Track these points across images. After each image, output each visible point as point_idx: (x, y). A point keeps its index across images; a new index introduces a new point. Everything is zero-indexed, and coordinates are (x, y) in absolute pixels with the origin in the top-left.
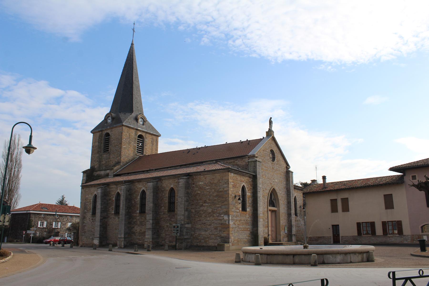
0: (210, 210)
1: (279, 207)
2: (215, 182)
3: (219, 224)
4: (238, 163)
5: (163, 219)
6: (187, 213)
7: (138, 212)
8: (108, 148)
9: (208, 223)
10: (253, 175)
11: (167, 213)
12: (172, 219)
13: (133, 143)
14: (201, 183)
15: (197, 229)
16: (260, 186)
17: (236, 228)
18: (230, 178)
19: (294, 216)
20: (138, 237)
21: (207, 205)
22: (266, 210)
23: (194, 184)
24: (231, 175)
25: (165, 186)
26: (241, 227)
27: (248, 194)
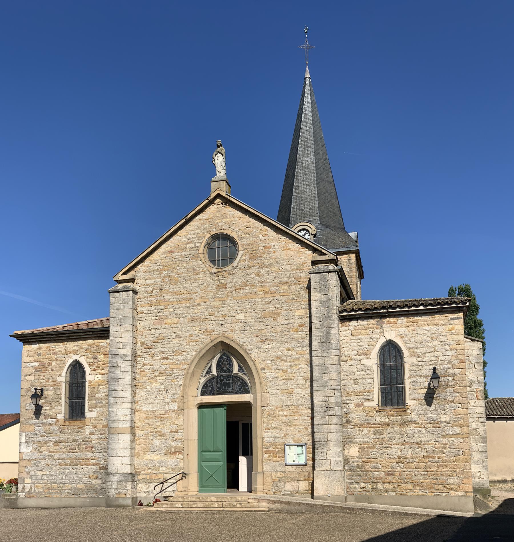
26: (64, 456)
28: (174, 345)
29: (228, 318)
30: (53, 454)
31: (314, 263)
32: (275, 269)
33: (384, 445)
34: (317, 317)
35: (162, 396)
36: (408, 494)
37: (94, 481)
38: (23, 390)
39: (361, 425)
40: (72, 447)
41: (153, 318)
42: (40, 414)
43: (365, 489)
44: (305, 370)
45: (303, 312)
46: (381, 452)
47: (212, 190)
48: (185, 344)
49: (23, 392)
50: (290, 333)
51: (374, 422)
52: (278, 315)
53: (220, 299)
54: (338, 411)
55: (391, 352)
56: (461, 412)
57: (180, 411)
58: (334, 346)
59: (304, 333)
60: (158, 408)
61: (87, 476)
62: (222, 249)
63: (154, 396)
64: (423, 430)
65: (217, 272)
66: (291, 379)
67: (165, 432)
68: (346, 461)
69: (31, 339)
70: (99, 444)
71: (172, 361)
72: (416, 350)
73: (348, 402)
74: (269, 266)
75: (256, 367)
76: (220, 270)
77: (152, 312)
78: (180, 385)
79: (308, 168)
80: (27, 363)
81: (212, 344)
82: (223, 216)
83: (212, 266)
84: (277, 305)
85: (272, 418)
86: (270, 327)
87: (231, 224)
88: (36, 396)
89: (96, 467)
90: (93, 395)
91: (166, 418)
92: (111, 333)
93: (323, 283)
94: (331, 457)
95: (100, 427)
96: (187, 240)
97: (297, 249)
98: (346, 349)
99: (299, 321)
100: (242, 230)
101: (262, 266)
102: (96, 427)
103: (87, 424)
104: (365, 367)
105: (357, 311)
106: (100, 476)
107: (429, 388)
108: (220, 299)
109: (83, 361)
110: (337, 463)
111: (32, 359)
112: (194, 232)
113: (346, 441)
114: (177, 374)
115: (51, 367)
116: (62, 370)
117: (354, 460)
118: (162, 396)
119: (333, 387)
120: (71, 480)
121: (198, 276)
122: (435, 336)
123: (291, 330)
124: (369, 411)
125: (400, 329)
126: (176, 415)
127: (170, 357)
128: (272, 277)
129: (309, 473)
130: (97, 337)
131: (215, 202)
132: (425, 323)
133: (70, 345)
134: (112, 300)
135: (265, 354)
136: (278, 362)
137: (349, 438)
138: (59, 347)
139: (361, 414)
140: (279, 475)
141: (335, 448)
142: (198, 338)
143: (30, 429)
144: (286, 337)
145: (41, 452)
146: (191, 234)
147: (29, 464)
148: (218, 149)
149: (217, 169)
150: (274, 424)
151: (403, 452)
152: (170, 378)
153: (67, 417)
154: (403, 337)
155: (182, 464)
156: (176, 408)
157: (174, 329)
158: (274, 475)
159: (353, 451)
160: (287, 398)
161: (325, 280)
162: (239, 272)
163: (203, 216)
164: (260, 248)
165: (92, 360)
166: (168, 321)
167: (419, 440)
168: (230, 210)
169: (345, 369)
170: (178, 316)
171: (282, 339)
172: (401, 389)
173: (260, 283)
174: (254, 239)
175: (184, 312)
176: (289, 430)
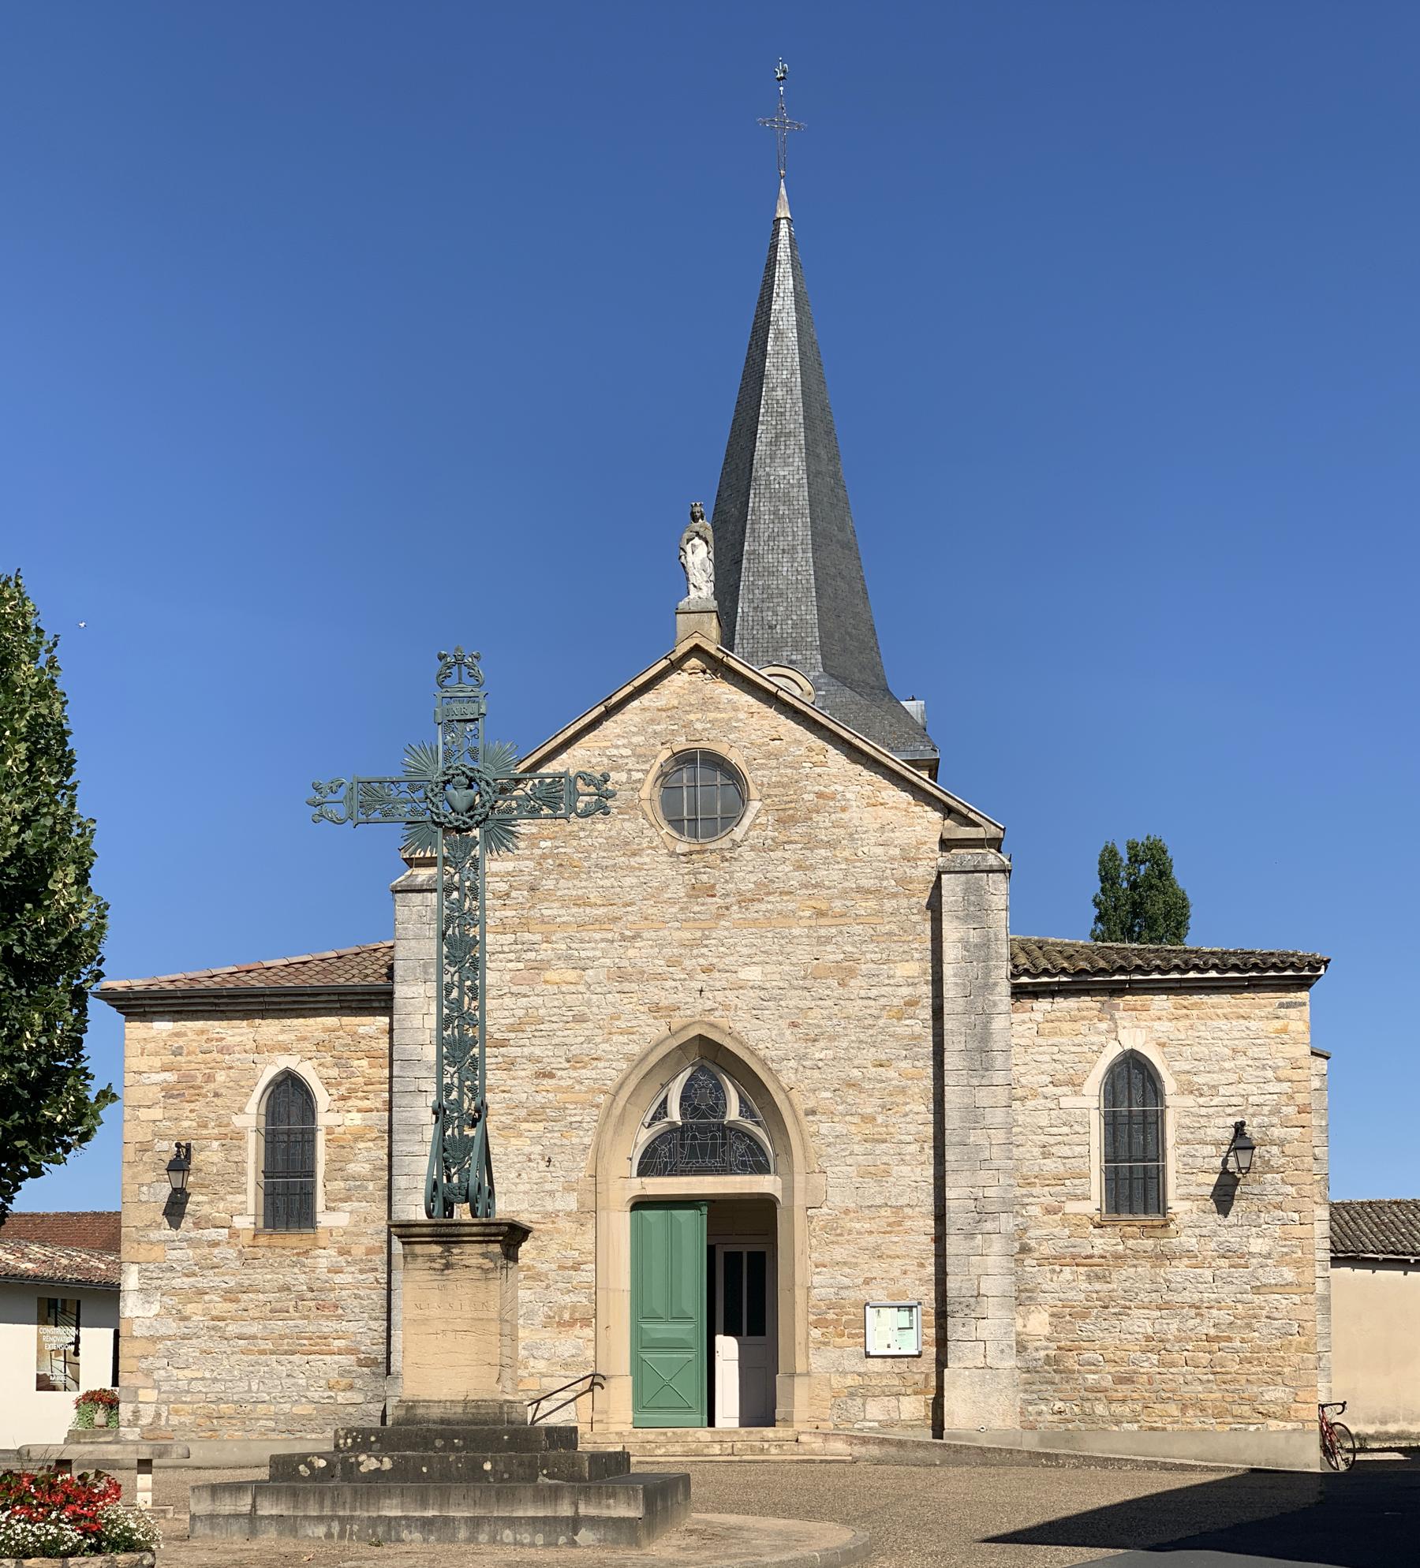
26: (254, 1329)
28: (567, 1041)
29: (717, 975)
30: (222, 1324)
31: (946, 844)
32: (846, 854)
33: (1114, 1308)
34: (956, 984)
35: (535, 1175)
36: (1169, 1427)
37: (341, 1397)
38: (130, 1148)
39: (1057, 1259)
40: (278, 1306)
41: (510, 965)
42: (182, 1215)
43: (1063, 1416)
44: (920, 1118)
45: (917, 967)
46: (1105, 1325)
47: (680, 635)
48: (598, 1040)
49: (130, 1153)
50: (881, 1022)
51: (1090, 1251)
52: (852, 973)
53: (697, 925)
54: (1007, 1223)
55: (1134, 1083)
56: (1298, 1231)
57: (591, 1212)
58: (999, 1060)
59: (920, 1023)
60: (525, 1206)
61: (322, 1383)
62: (703, 792)
63: (514, 1175)
64: (1208, 1274)
65: (691, 853)
66: (884, 1141)
67: (546, 1267)
68: (1021, 1348)
69: (151, 1006)
70: (357, 1297)
71: (562, 1083)
72: (1195, 1079)
73: (1026, 1200)
74: (829, 845)
75: (791, 1105)
76: (698, 848)
77: (506, 949)
78: (587, 1147)
79: (787, 500)
80: (140, 1073)
81: (675, 1043)
82: (707, 704)
83: (677, 836)
84: (849, 948)
85: (832, 1238)
86: (829, 1003)
87: (728, 727)
88: (180, 1163)
90: (338, 1165)
91: (548, 1232)
92: (398, 1002)
93: (972, 898)
94: (983, 1338)
95: (358, 1251)
96: (605, 761)
97: (904, 806)
98: (1022, 1069)
100: (759, 746)
101: (811, 843)
102: (349, 1253)
103: (322, 1243)
104: (1069, 1115)
105: (1055, 975)
106: (359, 1383)
107: (1225, 1172)
108: (697, 925)
109: (308, 1073)
110: (1002, 1351)
111: (157, 1062)
112: (625, 741)
113: (1023, 1297)
114: (578, 1118)
115: (212, 1086)
116: (247, 1095)
117: (1038, 1344)
118: (535, 1175)
119: (996, 1164)
120: (276, 1393)
121: (637, 858)
122: (1241, 1045)
123: (884, 1013)
124: (1075, 1224)
125: (1156, 1025)
126: (575, 1226)
127: (559, 1073)
128: (836, 875)
129: (927, 1375)
130: (349, 1008)
131: (685, 666)
132: (1219, 1011)
133: (270, 1029)
134: (401, 913)
135: (816, 1074)
136: (851, 1095)
137: (1026, 1290)
138: (235, 1032)
139: (1056, 1231)
140: (849, 1381)
141: (999, 1314)
142: (634, 1023)
143: (153, 1255)
144: (871, 1032)
146: (617, 747)
147: (151, 1348)
148: (696, 526)
149: (692, 579)
150: (839, 1253)
151: (1157, 1327)
152: (557, 1126)
153: (261, 1224)
154: (1163, 1045)
155: (590, 1353)
156: (574, 1206)
157: (568, 997)
158: (836, 1381)
159: (1038, 1323)
160: (871, 1186)
161: (979, 890)
162: (749, 855)
163: (651, 700)
164: (805, 796)
165: (334, 1072)
166: (550, 975)
167: (1197, 1296)
168: (725, 691)
169: (1021, 1119)
170: (582, 964)
171: (862, 1037)
172: (1154, 1172)
173: (807, 887)
174: (789, 771)
175: (598, 953)
176: (877, 1268)
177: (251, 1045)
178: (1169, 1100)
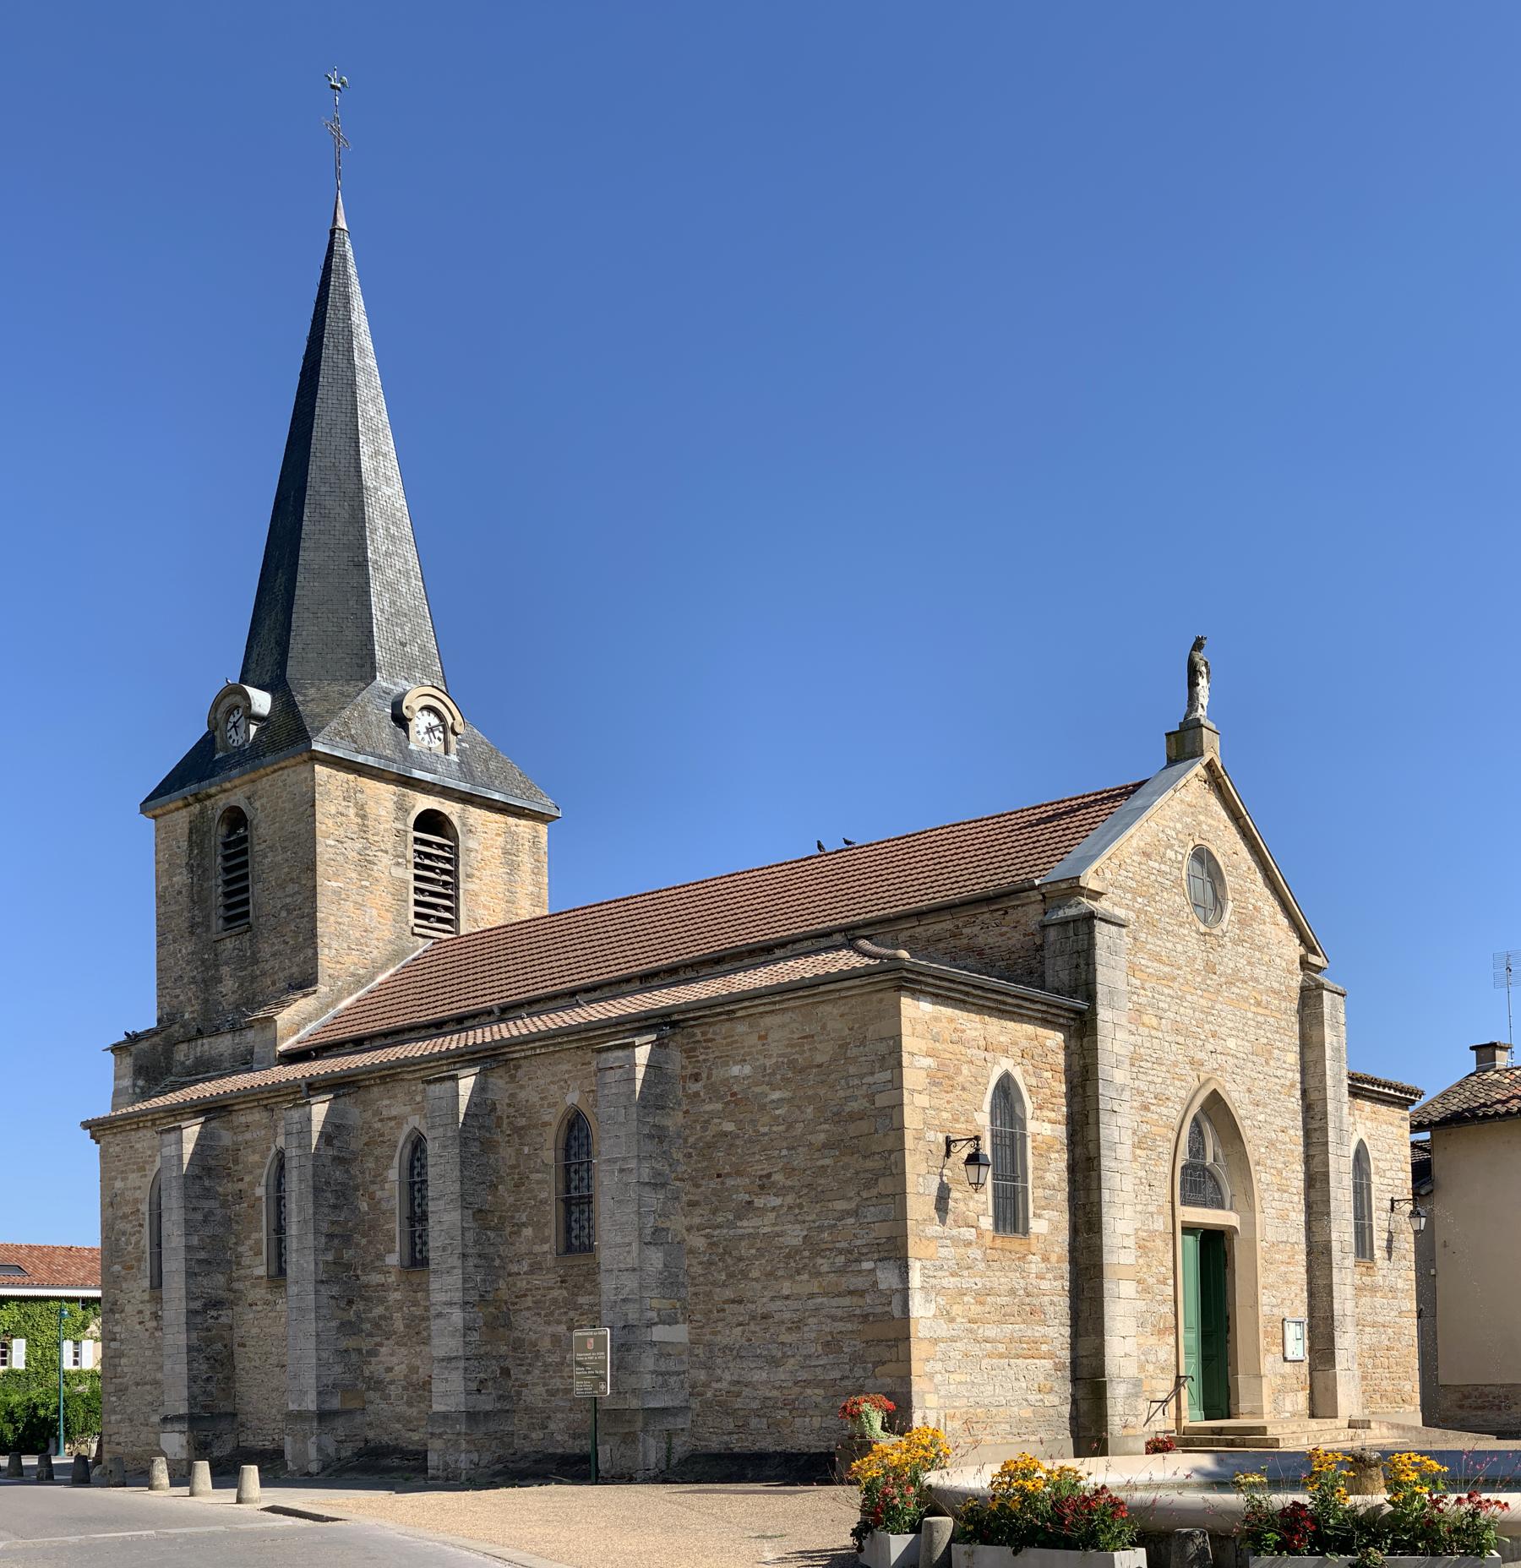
0: (794, 1236)
1: (1252, 1209)
2: (820, 1058)
3: (850, 1317)
4: (981, 941)
5: (529, 1301)
6: (656, 1258)
7: (393, 1259)
8: (246, 902)
9: (787, 1315)
10: (1079, 1013)
11: (550, 1260)
12: (581, 1300)
13: (386, 860)
14: (735, 1070)
15: (726, 1349)
16: (1120, 1076)
17: (953, 1340)
18: (906, 1029)
19: (1350, 1260)
20: (402, 1408)
21: (778, 1201)
22: (1161, 1224)
23: (696, 1078)
24: (916, 1012)
25: (535, 1098)
26: (991, 1331)
27: (1045, 1128)
30: (975, 1326)
89: (1048, 1364)
95: (1054, 1258)
99: (1290, 1075)
115: (960, 1079)
145: (952, 1320)
156: (1162, 1228)
165: (1033, 1081)
177: (982, 1043)
178: (1374, 1178)
